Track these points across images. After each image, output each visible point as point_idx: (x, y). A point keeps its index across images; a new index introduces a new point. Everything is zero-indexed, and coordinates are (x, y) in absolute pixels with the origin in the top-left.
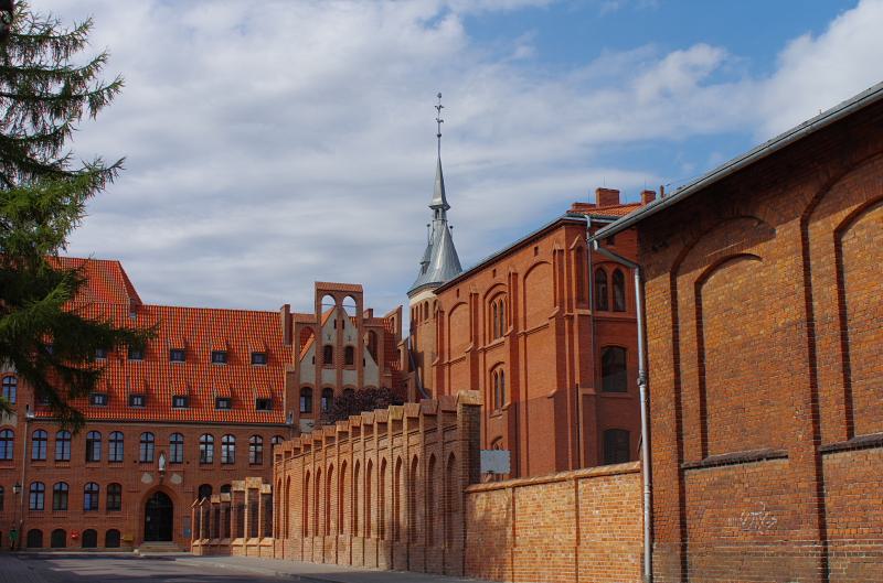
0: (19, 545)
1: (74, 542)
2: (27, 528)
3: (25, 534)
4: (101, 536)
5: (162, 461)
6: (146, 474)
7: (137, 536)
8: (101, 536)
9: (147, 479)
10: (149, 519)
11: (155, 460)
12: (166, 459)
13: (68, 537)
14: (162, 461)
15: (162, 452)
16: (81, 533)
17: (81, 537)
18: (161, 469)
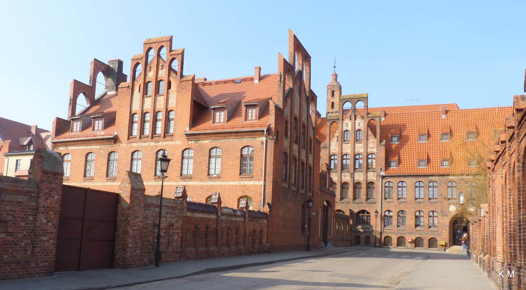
7: (448, 242)
9: (453, 209)
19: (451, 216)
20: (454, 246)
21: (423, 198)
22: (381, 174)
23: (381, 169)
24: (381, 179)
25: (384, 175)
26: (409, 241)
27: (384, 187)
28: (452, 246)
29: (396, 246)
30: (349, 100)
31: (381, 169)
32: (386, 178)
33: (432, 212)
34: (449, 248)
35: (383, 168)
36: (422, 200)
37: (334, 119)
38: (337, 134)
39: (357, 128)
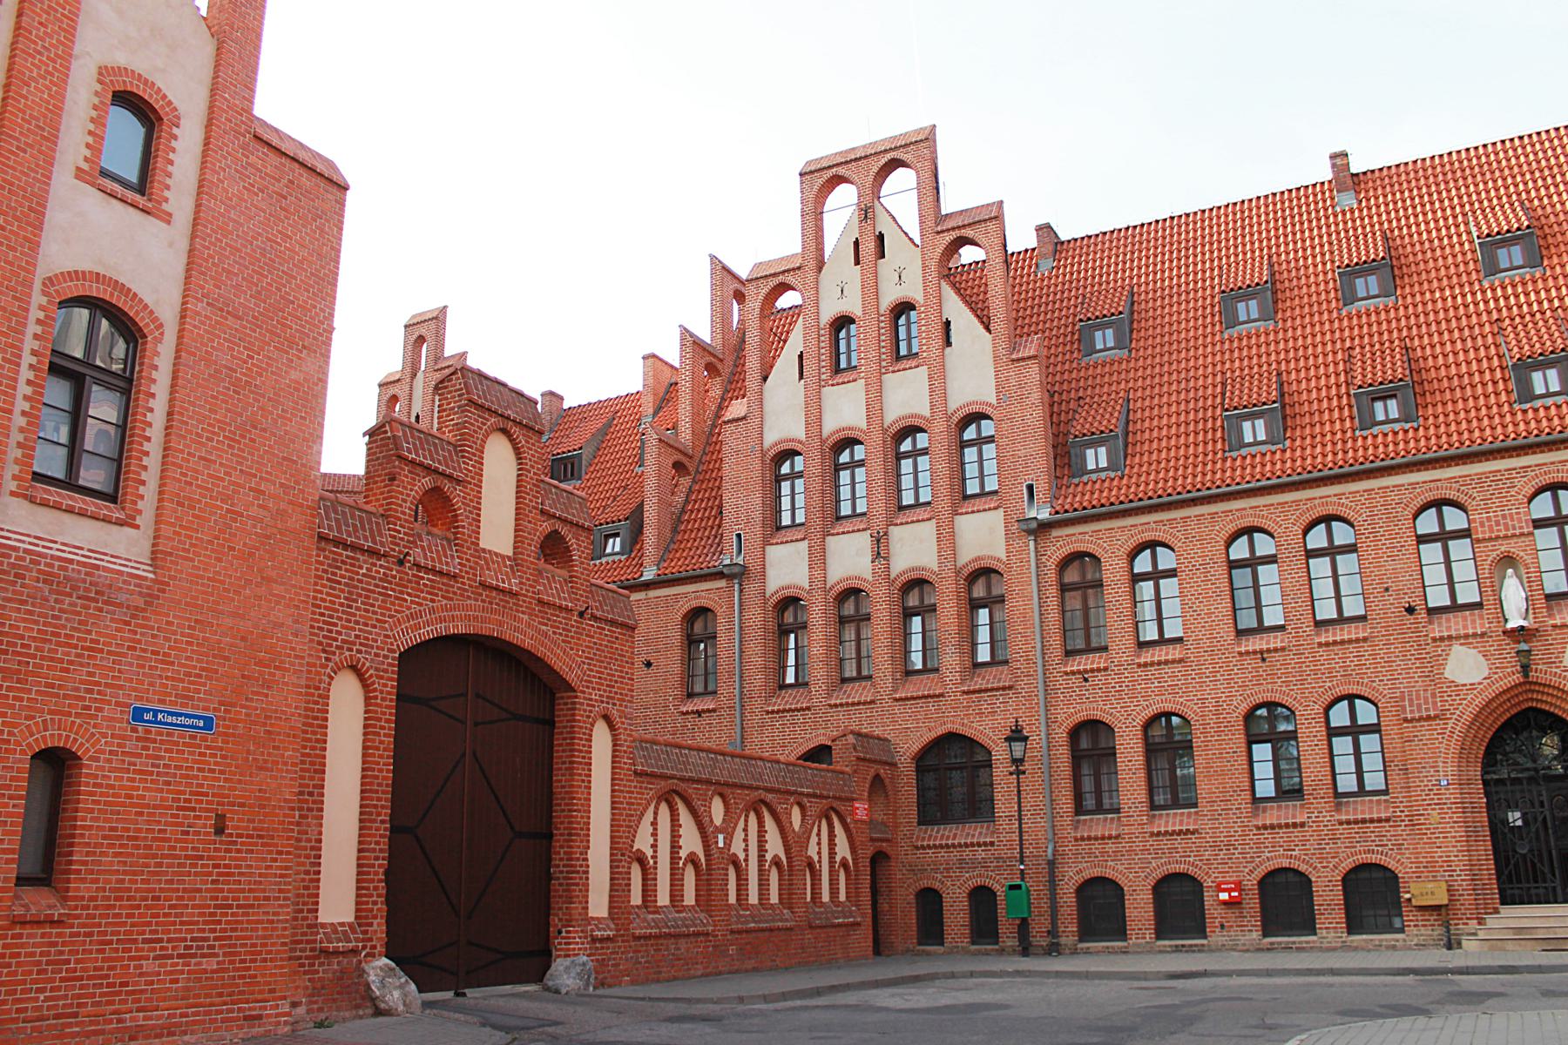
0: (1053, 932)
1: (1231, 914)
2: (1072, 875)
3: (1068, 899)
4: (1328, 894)
5: (1513, 594)
6: (1458, 650)
7: (1462, 881)
8: (1328, 894)
10: (1515, 818)
11: (1489, 601)
12: (1532, 584)
13: (1208, 896)
14: (1513, 594)
15: (1508, 560)
16: (1251, 882)
17: (1253, 902)
18: (1513, 624)
19: (1467, 709)
20: (1508, 911)
21: (1281, 628)
22: (1032, 514)
23: (1030, 488)
24: (1032, 544)
25: (1044, 514)
26: (1224, 896)
27: (1052, 591)
28: (1496, 911)
29: (1149, 935)
30: (841, 171)
31: (1030, 488)
32: (1055, 533)
33: (1346, 703)
34: (1481, 921)
35: (1041, 488)
36: (1275, 641)
37: (774, 275)
38: (796, 342)
39: (890, 295)
